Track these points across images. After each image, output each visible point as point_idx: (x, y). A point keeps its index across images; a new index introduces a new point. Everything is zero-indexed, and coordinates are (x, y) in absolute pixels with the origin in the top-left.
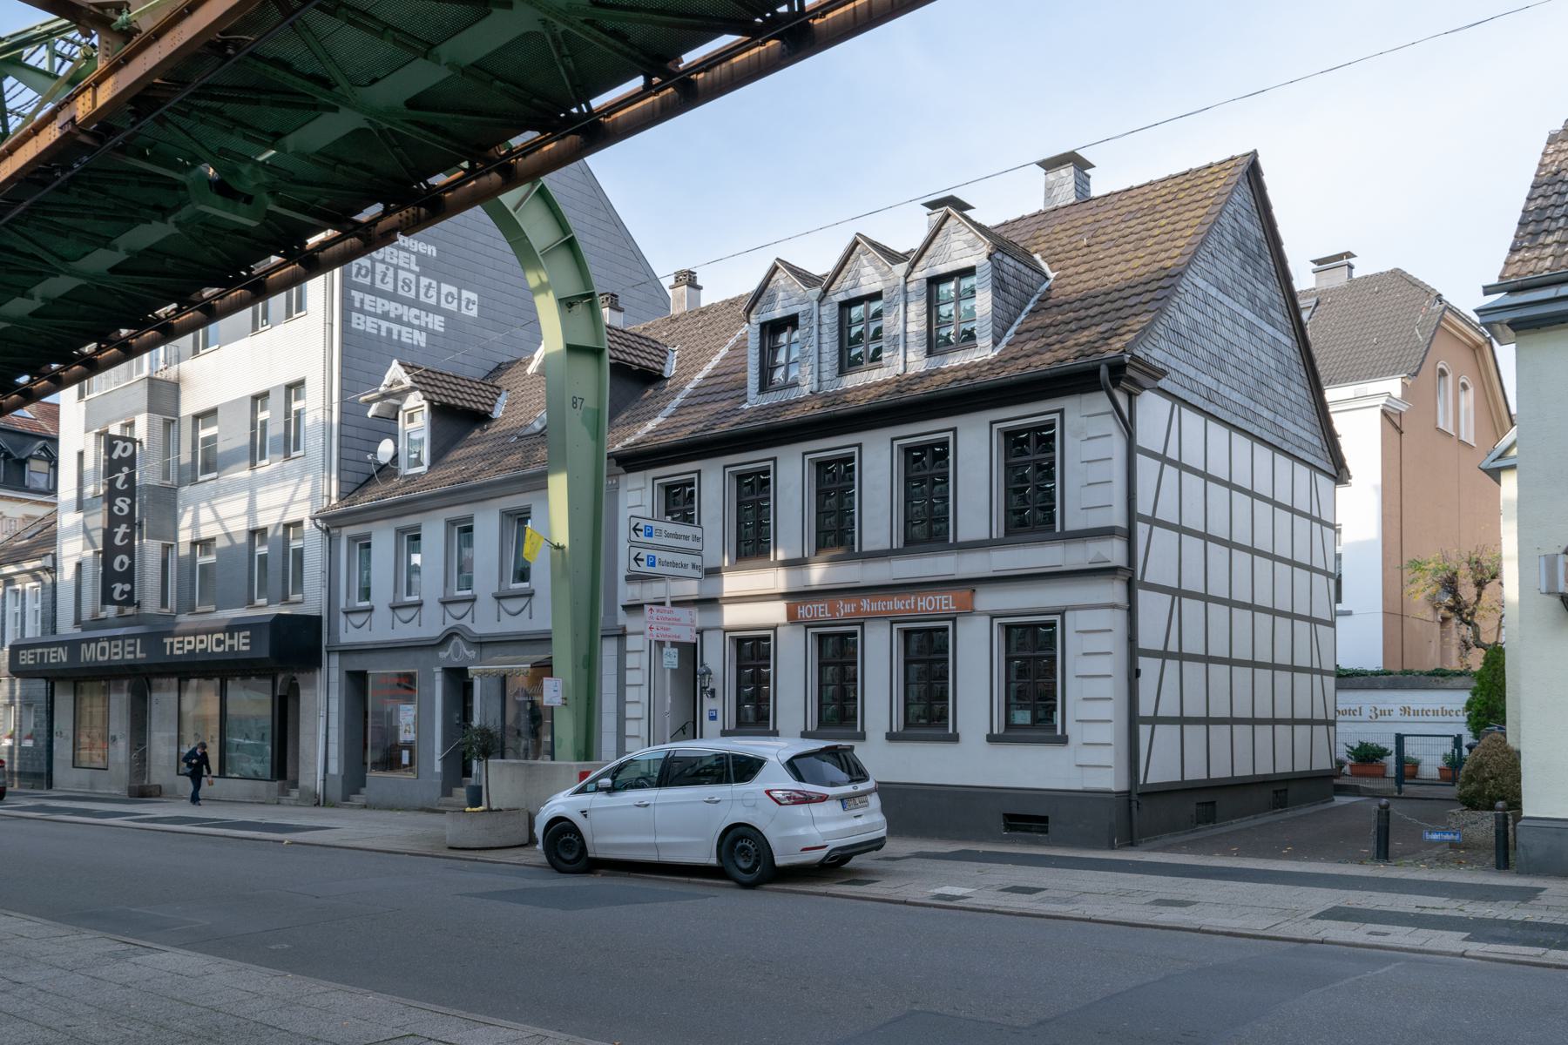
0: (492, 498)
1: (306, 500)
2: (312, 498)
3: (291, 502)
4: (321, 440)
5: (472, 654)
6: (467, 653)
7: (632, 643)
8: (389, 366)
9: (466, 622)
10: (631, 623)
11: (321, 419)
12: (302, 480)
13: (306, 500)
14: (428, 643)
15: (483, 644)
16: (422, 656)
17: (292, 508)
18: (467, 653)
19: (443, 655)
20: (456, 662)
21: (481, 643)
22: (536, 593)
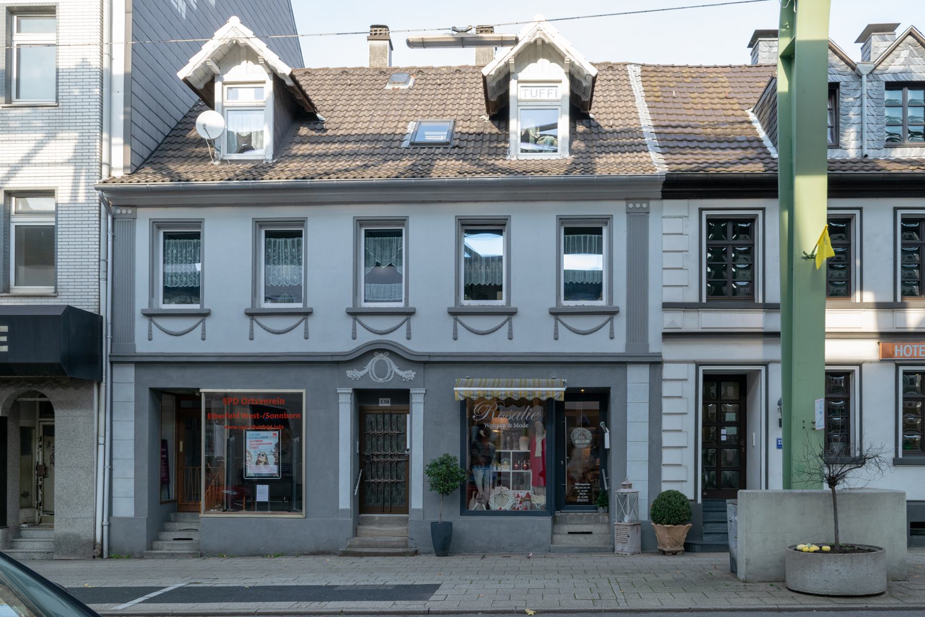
0: (440, 202)
1: (68, 162)
2: (78, 161)
3: (26, 161)
4: (97, 91)
5: (409, 374)
6: (401, 373)
7: (668, 371)
8: (225, 21)
9: (398, 337)
10: (669, 351)
11: (95, 63)
12: (51, 136)
13: (68, 162)
14: (329, 359)
15: (426, 363)
16: (324, 374)
17: (26, 171)
18: (401, 373)
19: (353, 373)
20: (380, 382)
21: (425, 363)
22: (520, 311)
